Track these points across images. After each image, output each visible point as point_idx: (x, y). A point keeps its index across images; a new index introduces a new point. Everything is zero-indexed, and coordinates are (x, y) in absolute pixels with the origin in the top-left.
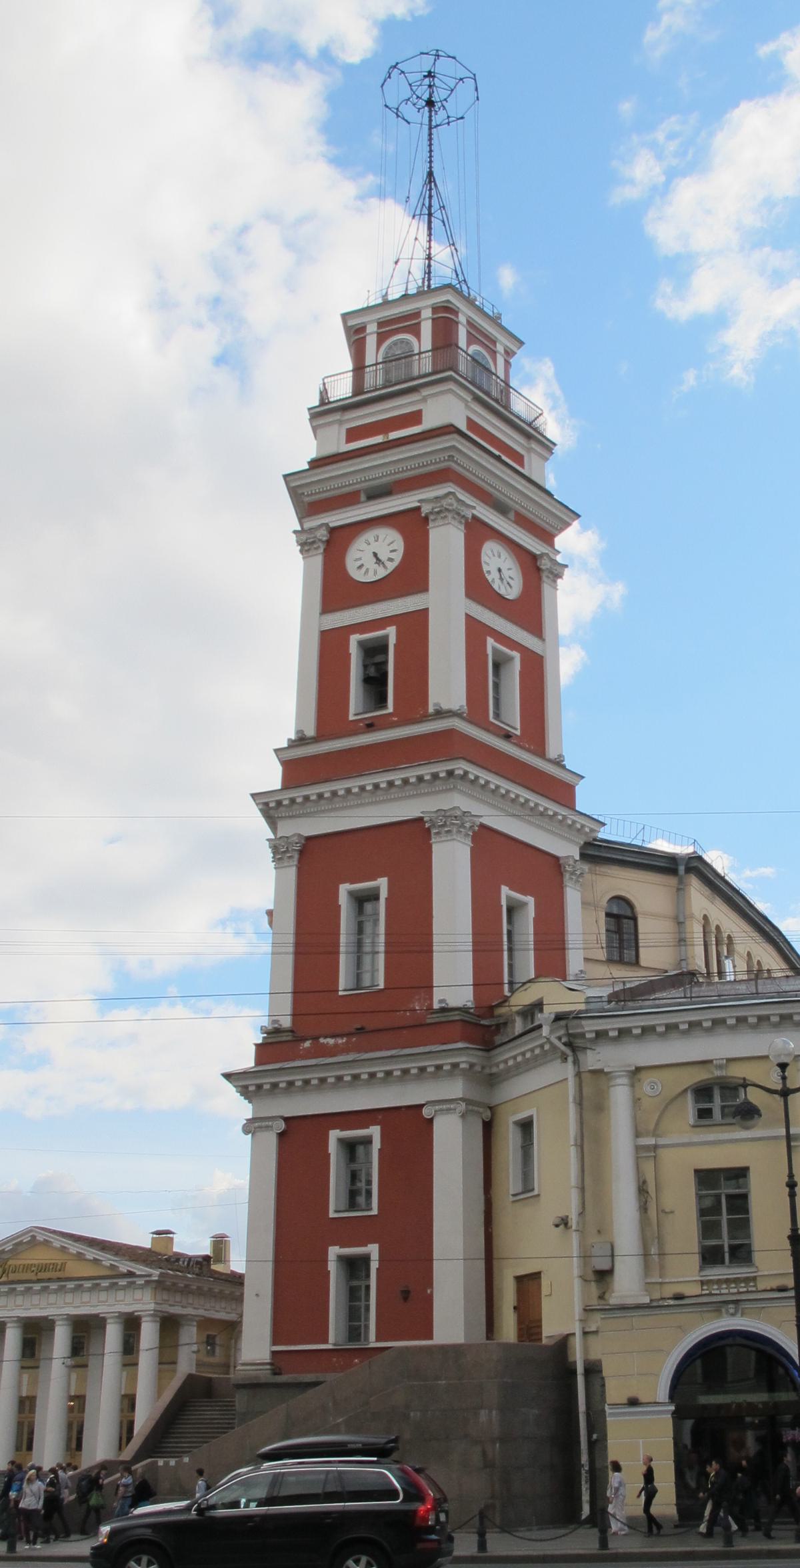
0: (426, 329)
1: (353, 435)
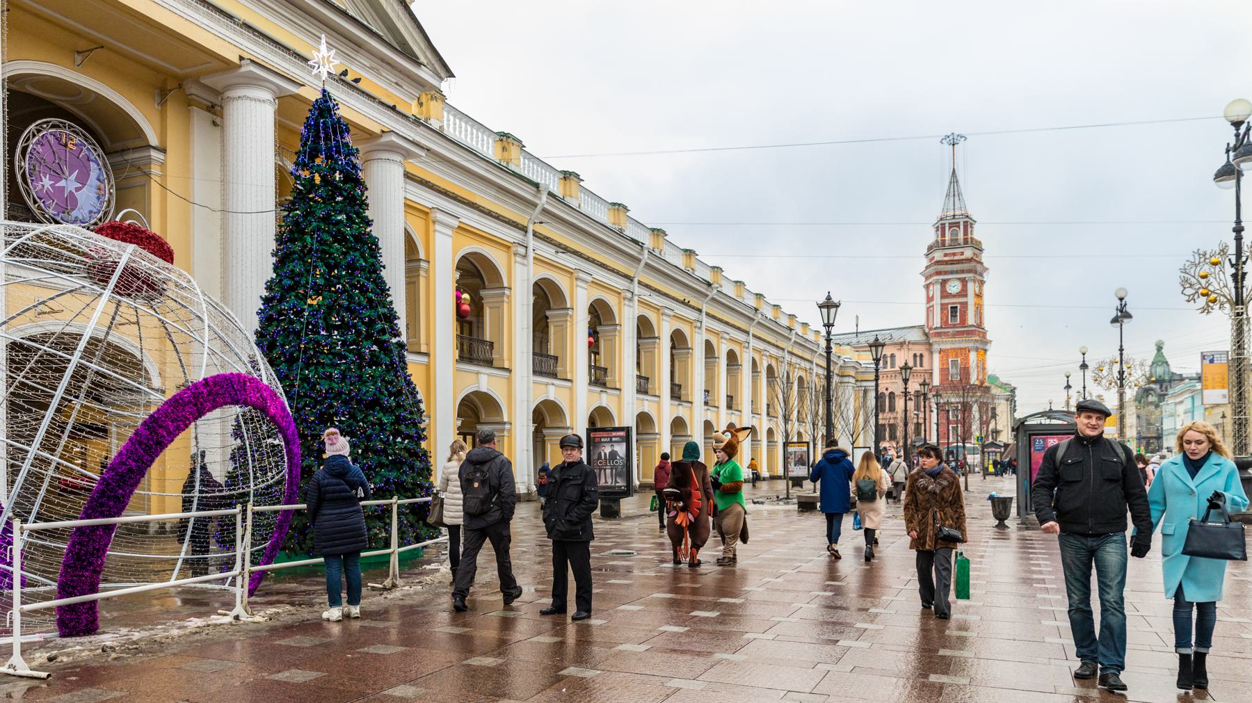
0: (962, 227)
1: (946, 255)
